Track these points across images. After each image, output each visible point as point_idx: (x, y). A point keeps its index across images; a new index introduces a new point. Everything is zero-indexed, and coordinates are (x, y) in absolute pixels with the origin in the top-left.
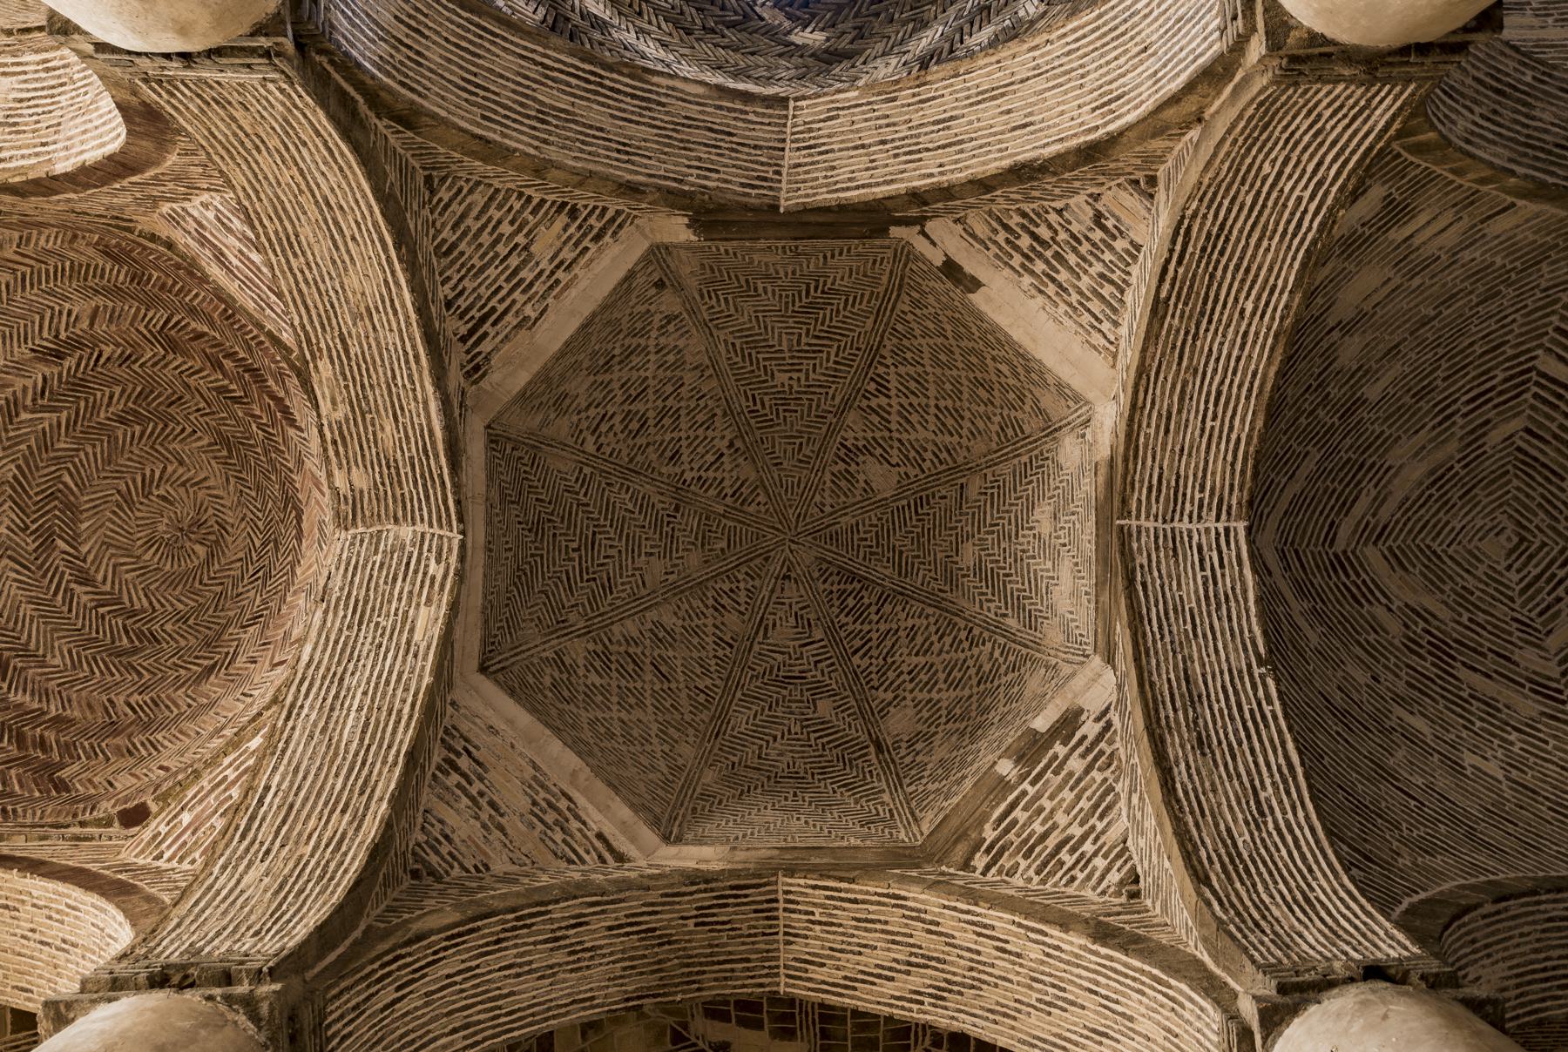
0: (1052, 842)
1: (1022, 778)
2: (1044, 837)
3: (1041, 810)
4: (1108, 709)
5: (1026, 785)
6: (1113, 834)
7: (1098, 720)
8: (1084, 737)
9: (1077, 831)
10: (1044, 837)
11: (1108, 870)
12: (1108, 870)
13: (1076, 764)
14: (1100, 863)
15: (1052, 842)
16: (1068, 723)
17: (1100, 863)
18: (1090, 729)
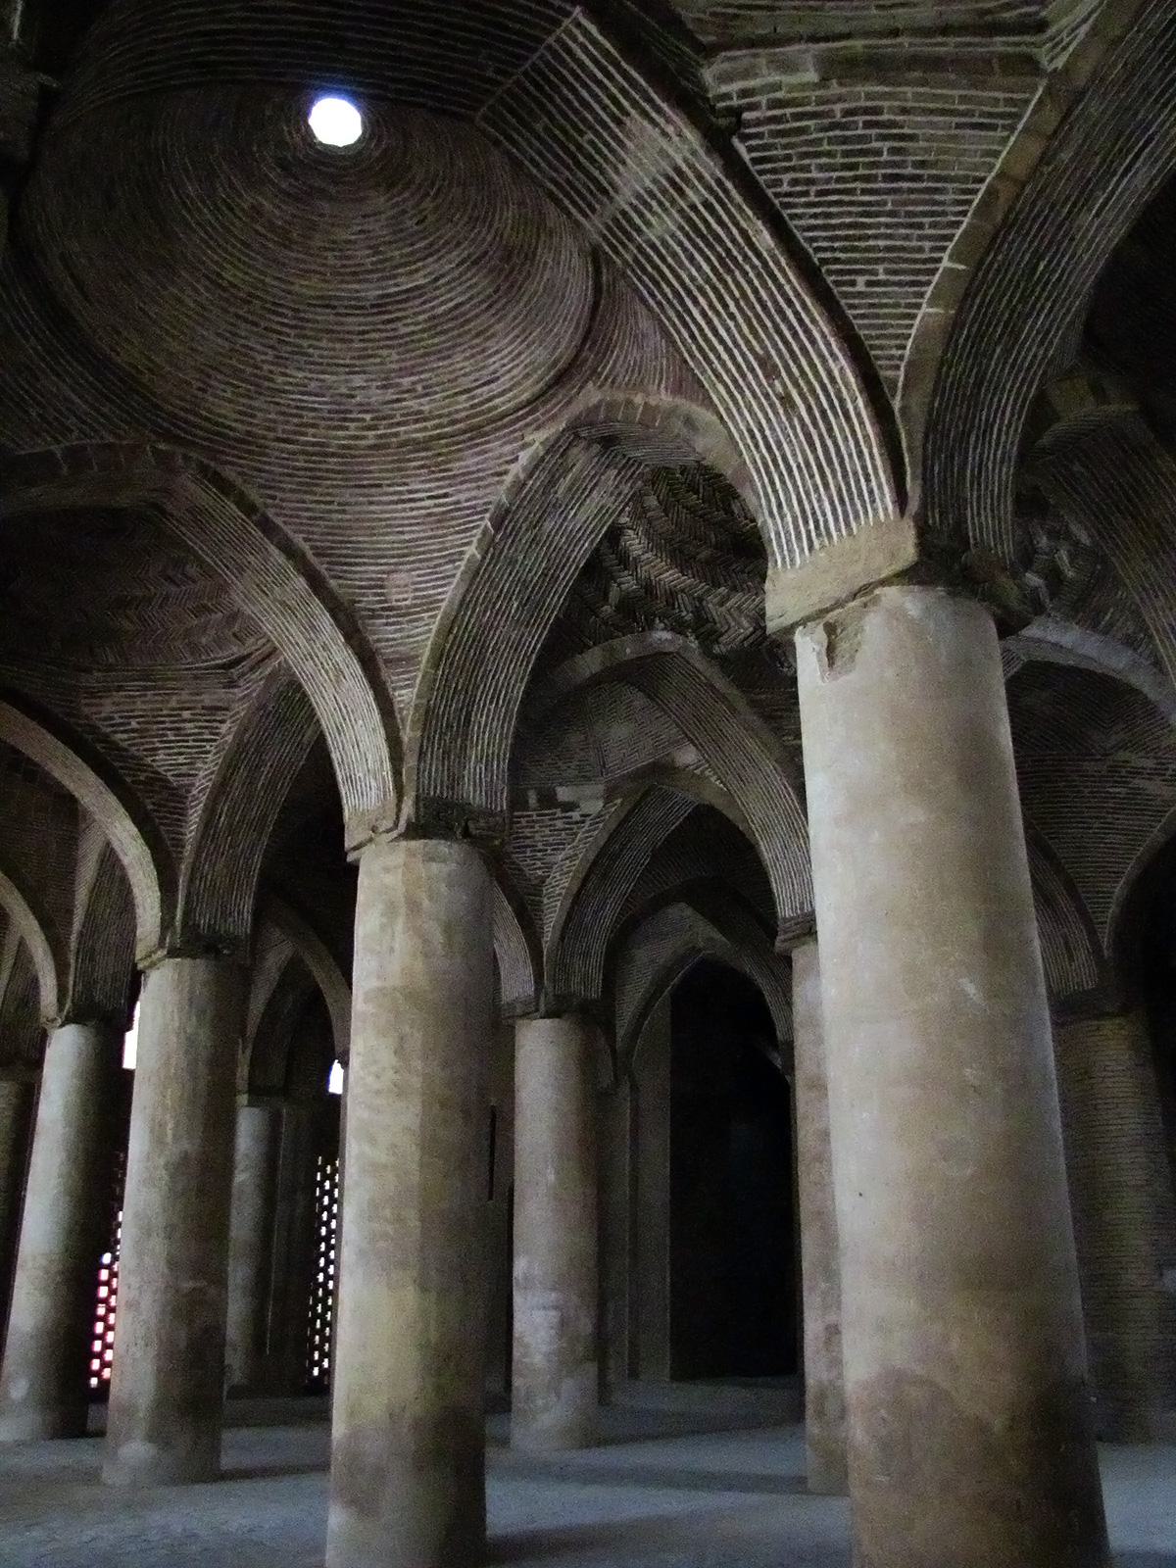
0: (528, 842)
1: (535, 810)
2: (528, 838)
3: (532, 827)
4: (589, 815)
5: (534, 813)
6: (548, 859)
7: (582, 816)
8: (571, 817)
9: (540, 846)
10: (528, 838)
11: (540, 868)
12: (540, 868)
13: (559, 824)
14: (539, 864)
15: (528, 842)
16: (570, 806)
17: (539, 864)
18: (576, 815)
